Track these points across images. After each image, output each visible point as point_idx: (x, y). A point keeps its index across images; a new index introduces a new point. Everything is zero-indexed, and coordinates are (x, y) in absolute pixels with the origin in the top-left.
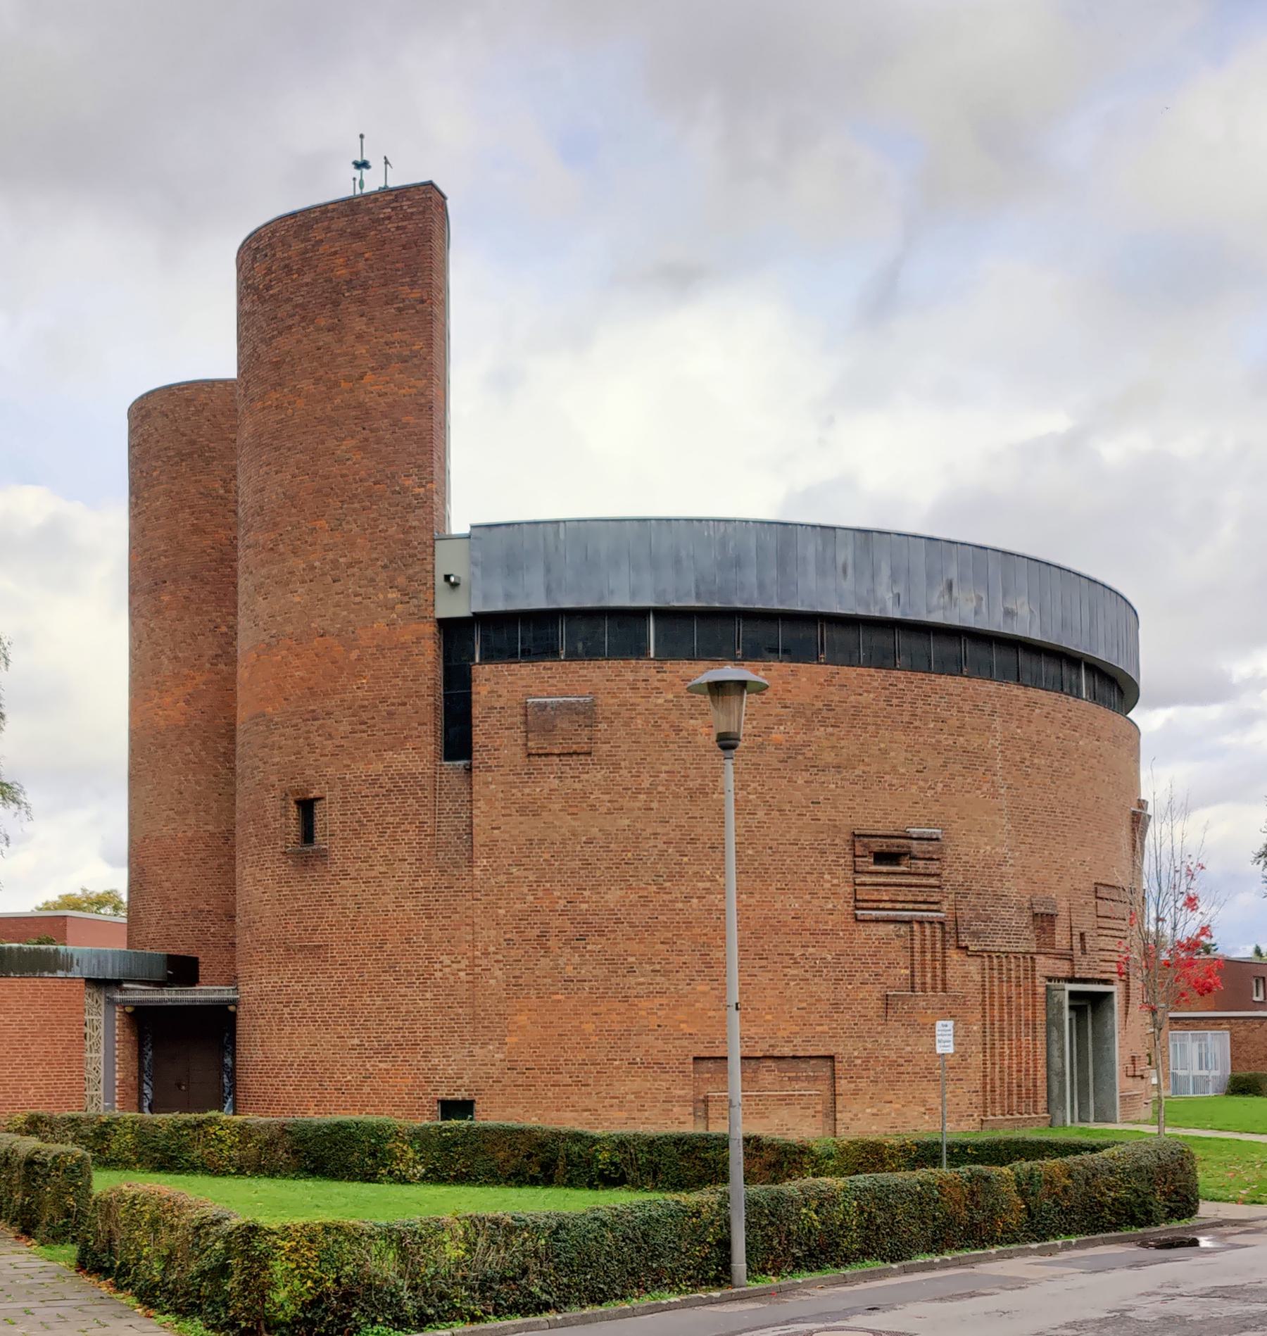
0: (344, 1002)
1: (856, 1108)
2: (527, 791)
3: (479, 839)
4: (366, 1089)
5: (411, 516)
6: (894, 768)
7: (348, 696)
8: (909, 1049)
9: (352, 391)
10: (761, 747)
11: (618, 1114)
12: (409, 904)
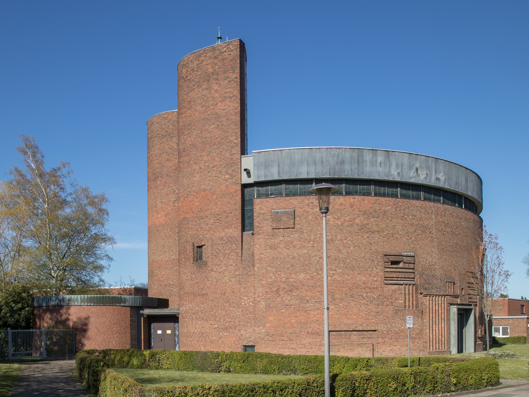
0: (213, 313)
1: (384, 348)
2: (272, 241)
3: (257, 258)
4: (220, 342)
5: (233, 150)
6: (398, 232)
7: (213, 211)
9: (214, 109)
10: (352, 225)
11: (303, 350)
12: (233, 280)
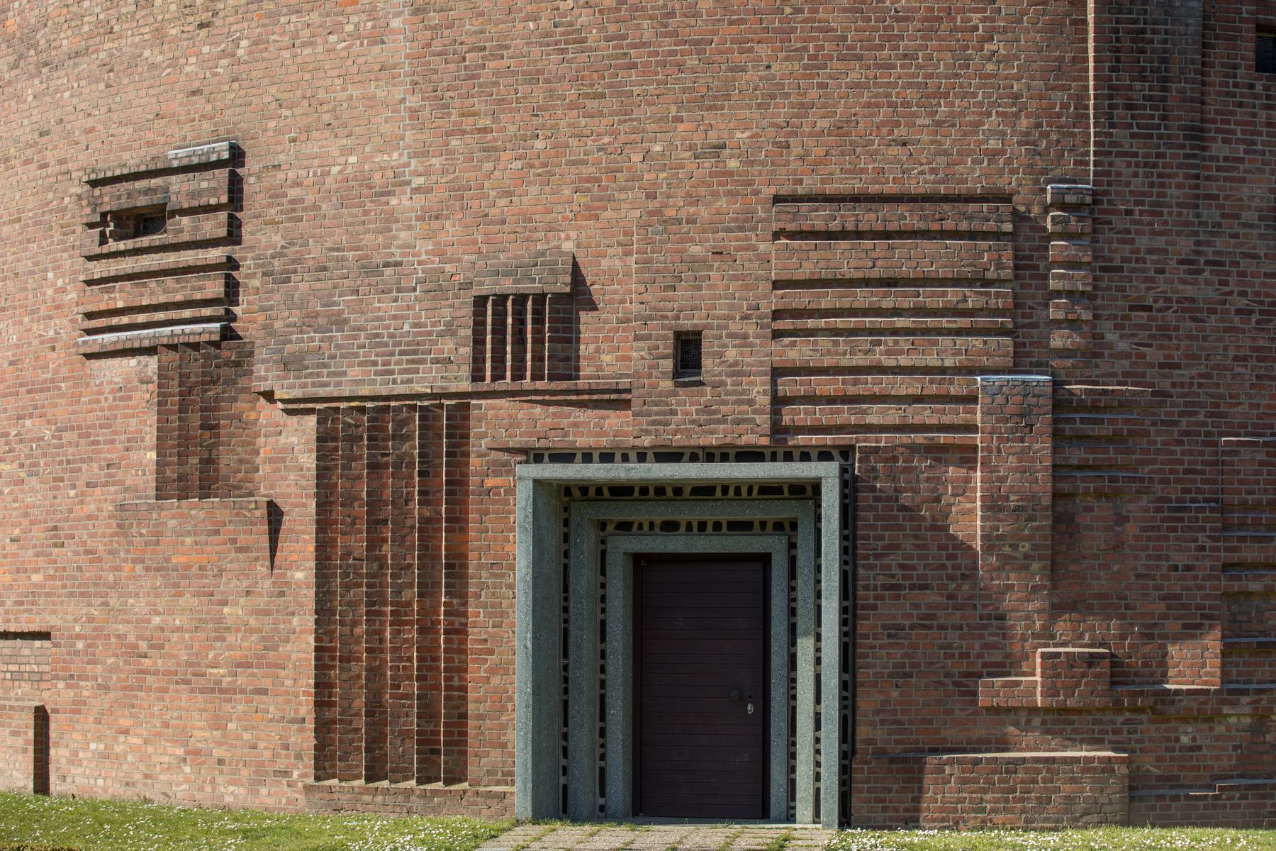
8: (157, 620)
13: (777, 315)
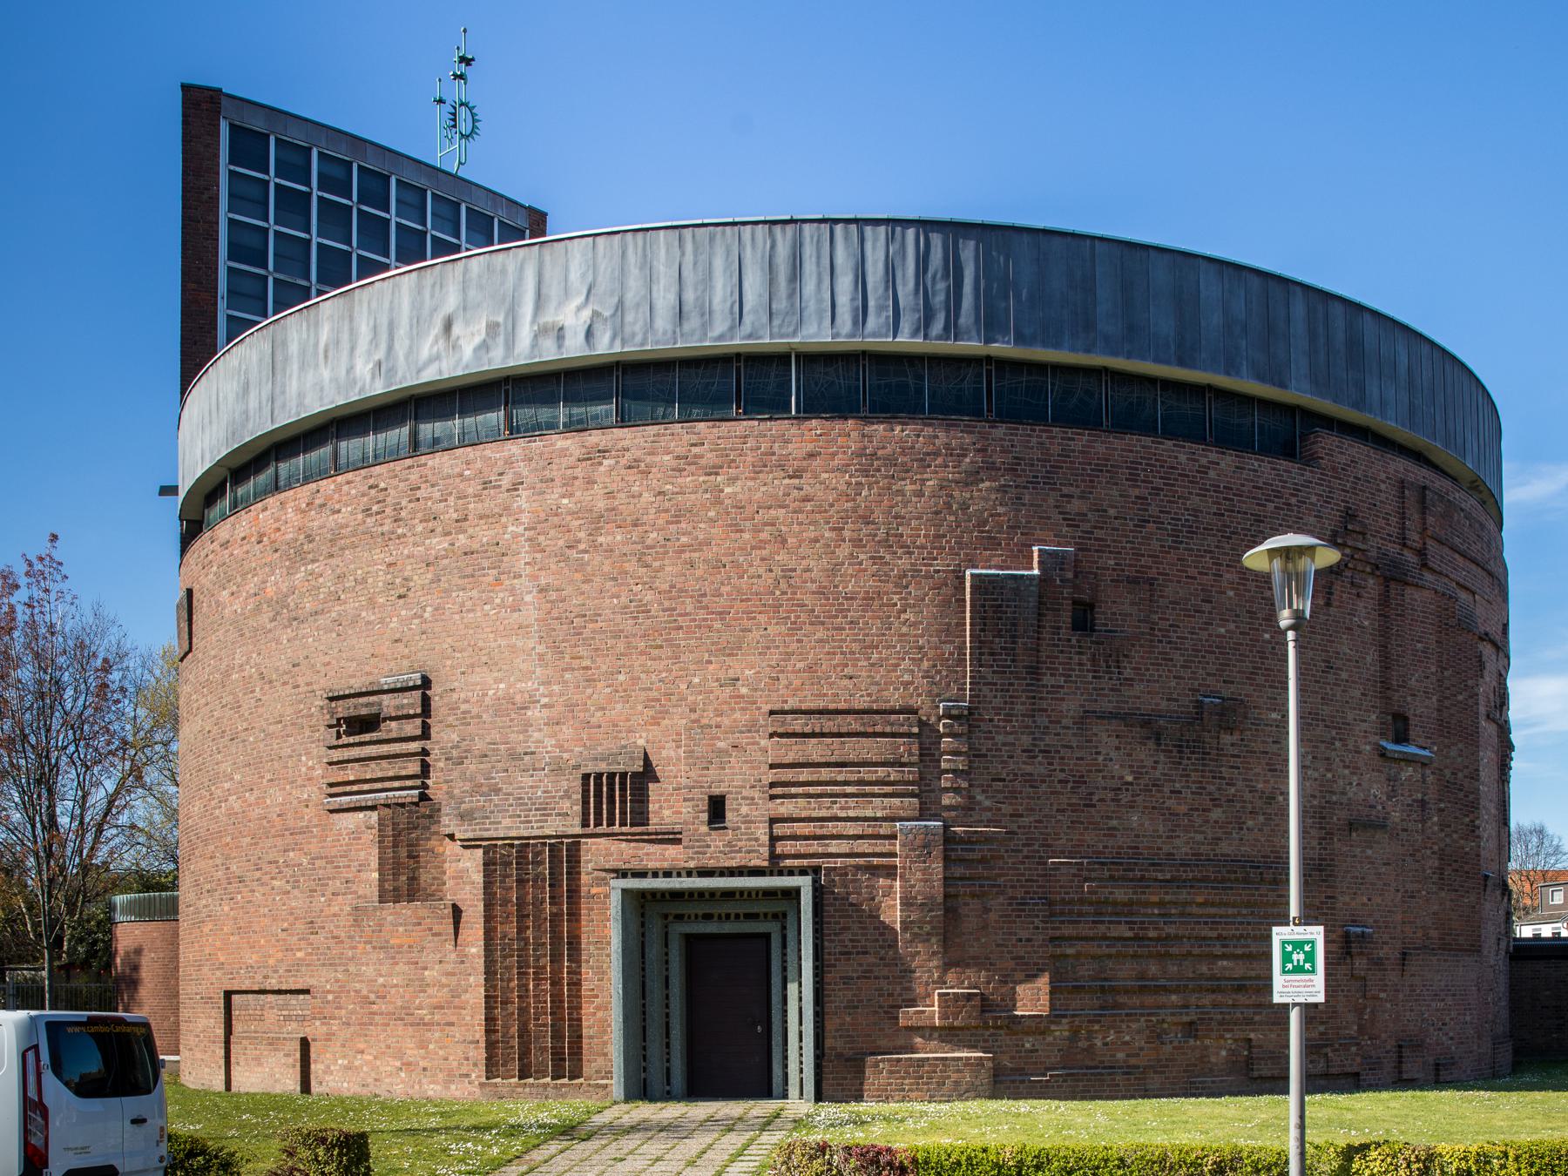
8: (381, 980)
13: (772, 785)
